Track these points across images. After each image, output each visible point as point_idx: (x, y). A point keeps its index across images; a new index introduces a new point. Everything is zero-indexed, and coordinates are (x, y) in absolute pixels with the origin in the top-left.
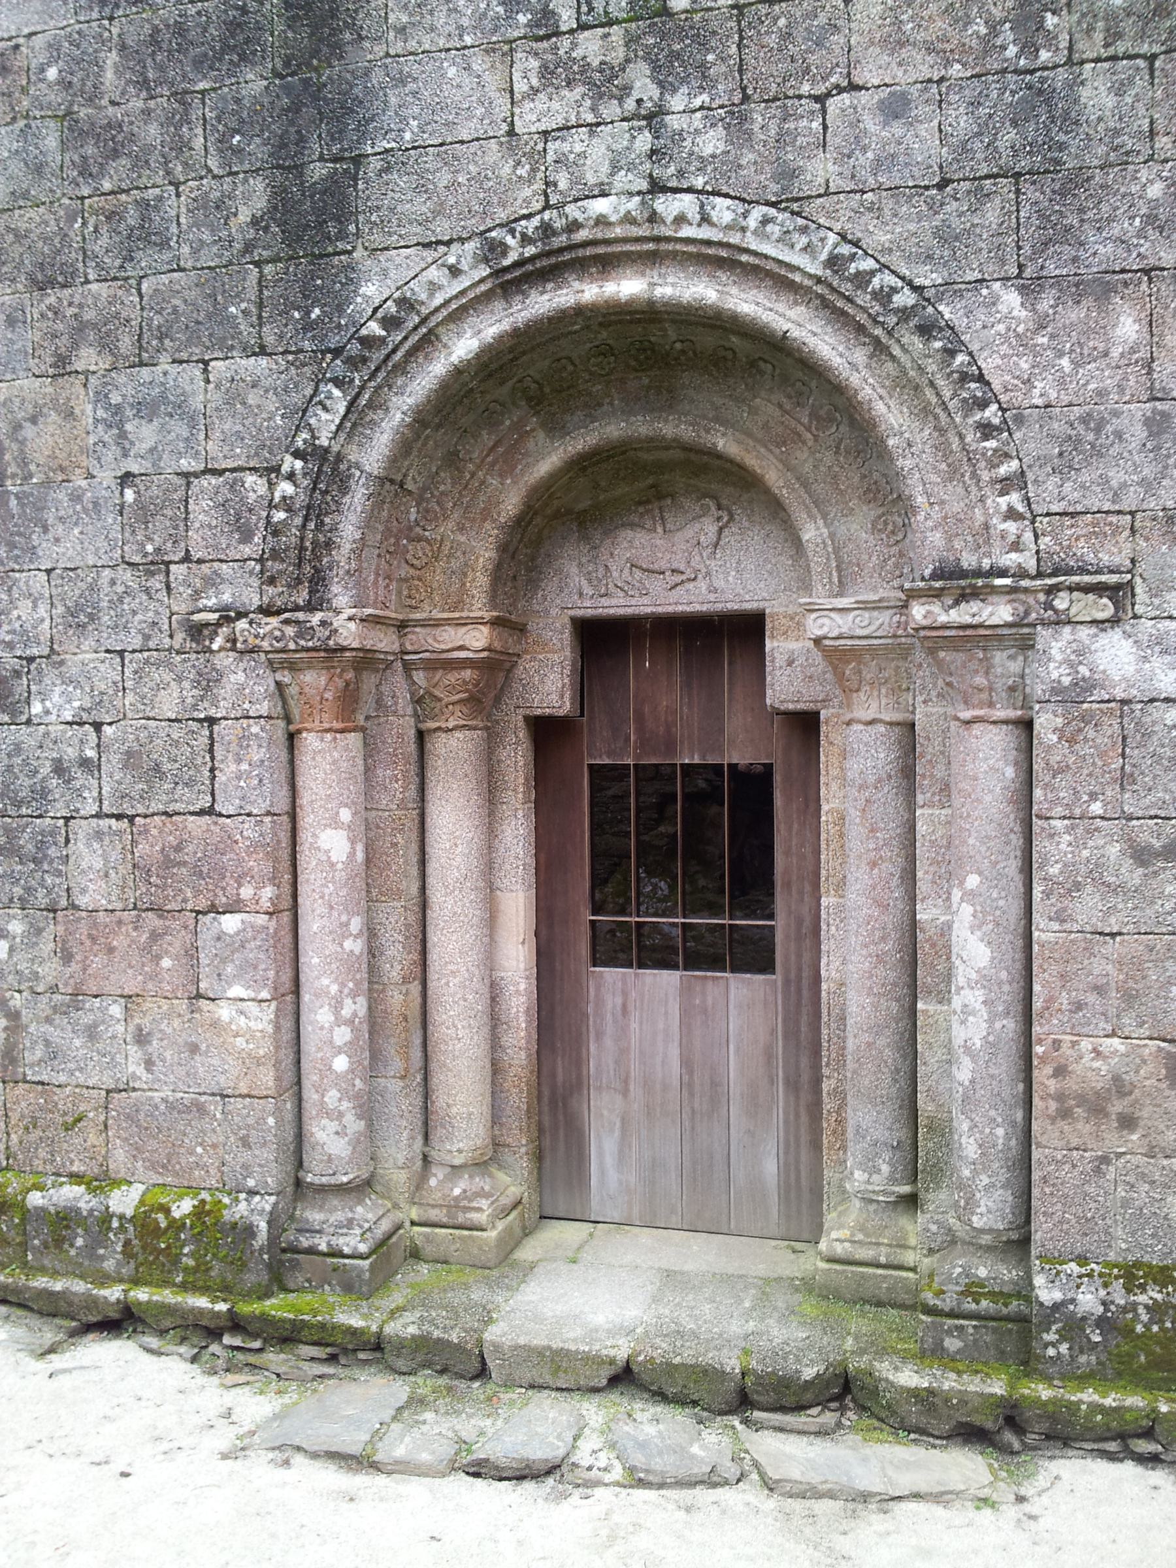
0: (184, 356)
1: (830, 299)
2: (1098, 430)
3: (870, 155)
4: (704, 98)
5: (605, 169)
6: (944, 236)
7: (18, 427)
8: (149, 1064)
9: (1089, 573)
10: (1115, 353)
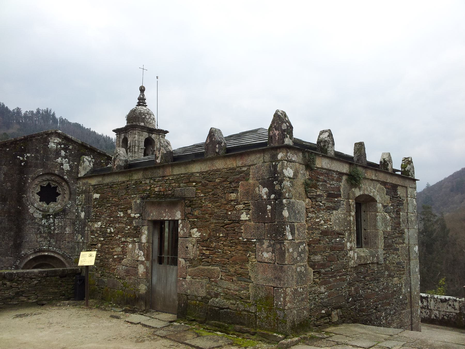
1: (63, 256)
6: (71, 252)
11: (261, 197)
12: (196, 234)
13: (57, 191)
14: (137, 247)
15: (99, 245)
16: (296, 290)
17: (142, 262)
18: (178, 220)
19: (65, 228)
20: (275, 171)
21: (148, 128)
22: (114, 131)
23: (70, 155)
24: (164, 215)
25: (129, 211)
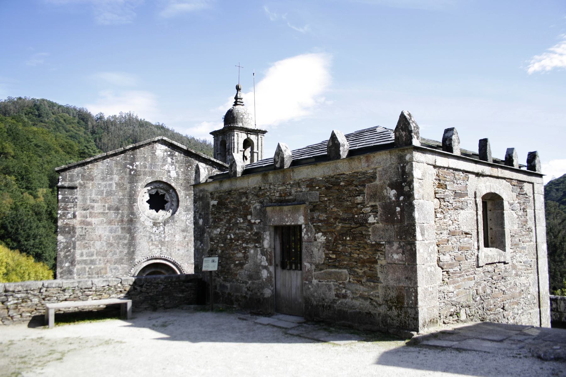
1: (174, 263)
11: (390, 199)
12: (321, 238)
13: (165, 199)
14: (259, 252)
15: (220, 251)
16: (426, 289)
17: (265, 267)
18: (301, 226)
20: (404, 172)
21: (247, 129)
22: (211, 133)
23: (176, 162)
24: (286, 220)
25: (249, 217)
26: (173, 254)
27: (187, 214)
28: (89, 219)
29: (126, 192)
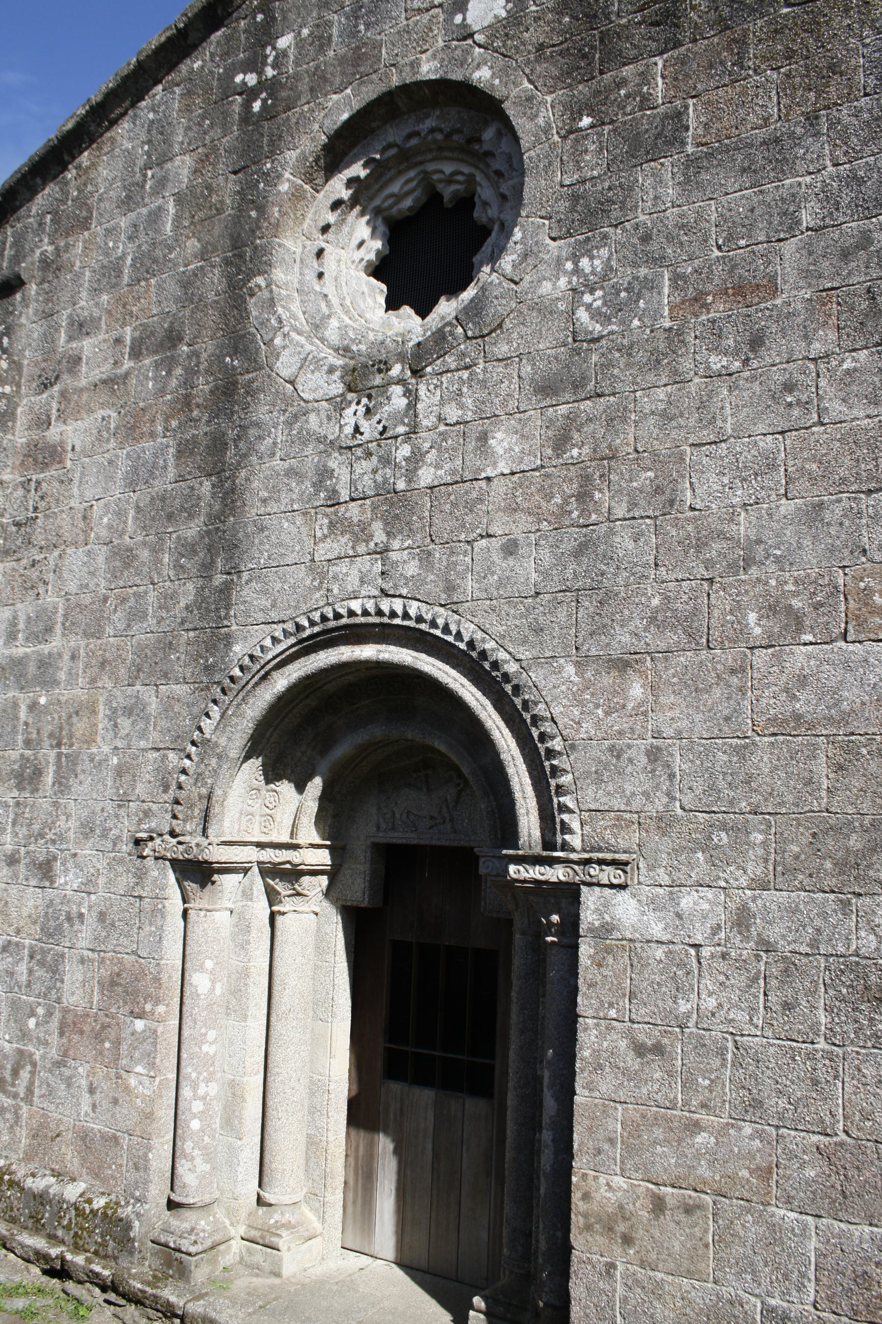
0: (148, 682)
2: (618, 757)
3: (495, 577)
4: (410, 542)
5: (357, 582)
7: (70, 717)
8: (94, 1106)
9: (611, 851)
10: (630, 705)
19: (484, 437)
26: (470, 585)
27: (584, 249)
28: (53, 433)
29: (217, 231)
